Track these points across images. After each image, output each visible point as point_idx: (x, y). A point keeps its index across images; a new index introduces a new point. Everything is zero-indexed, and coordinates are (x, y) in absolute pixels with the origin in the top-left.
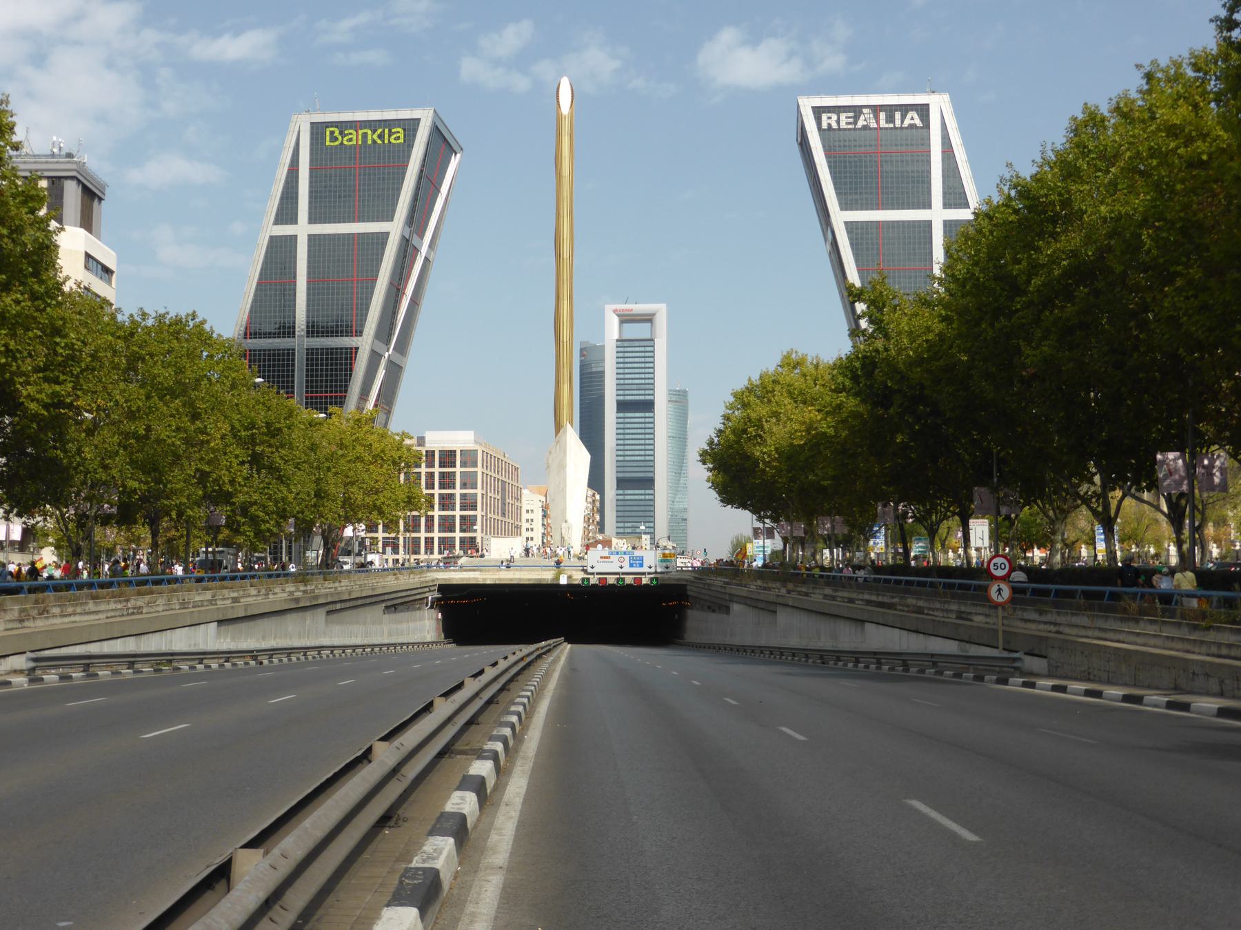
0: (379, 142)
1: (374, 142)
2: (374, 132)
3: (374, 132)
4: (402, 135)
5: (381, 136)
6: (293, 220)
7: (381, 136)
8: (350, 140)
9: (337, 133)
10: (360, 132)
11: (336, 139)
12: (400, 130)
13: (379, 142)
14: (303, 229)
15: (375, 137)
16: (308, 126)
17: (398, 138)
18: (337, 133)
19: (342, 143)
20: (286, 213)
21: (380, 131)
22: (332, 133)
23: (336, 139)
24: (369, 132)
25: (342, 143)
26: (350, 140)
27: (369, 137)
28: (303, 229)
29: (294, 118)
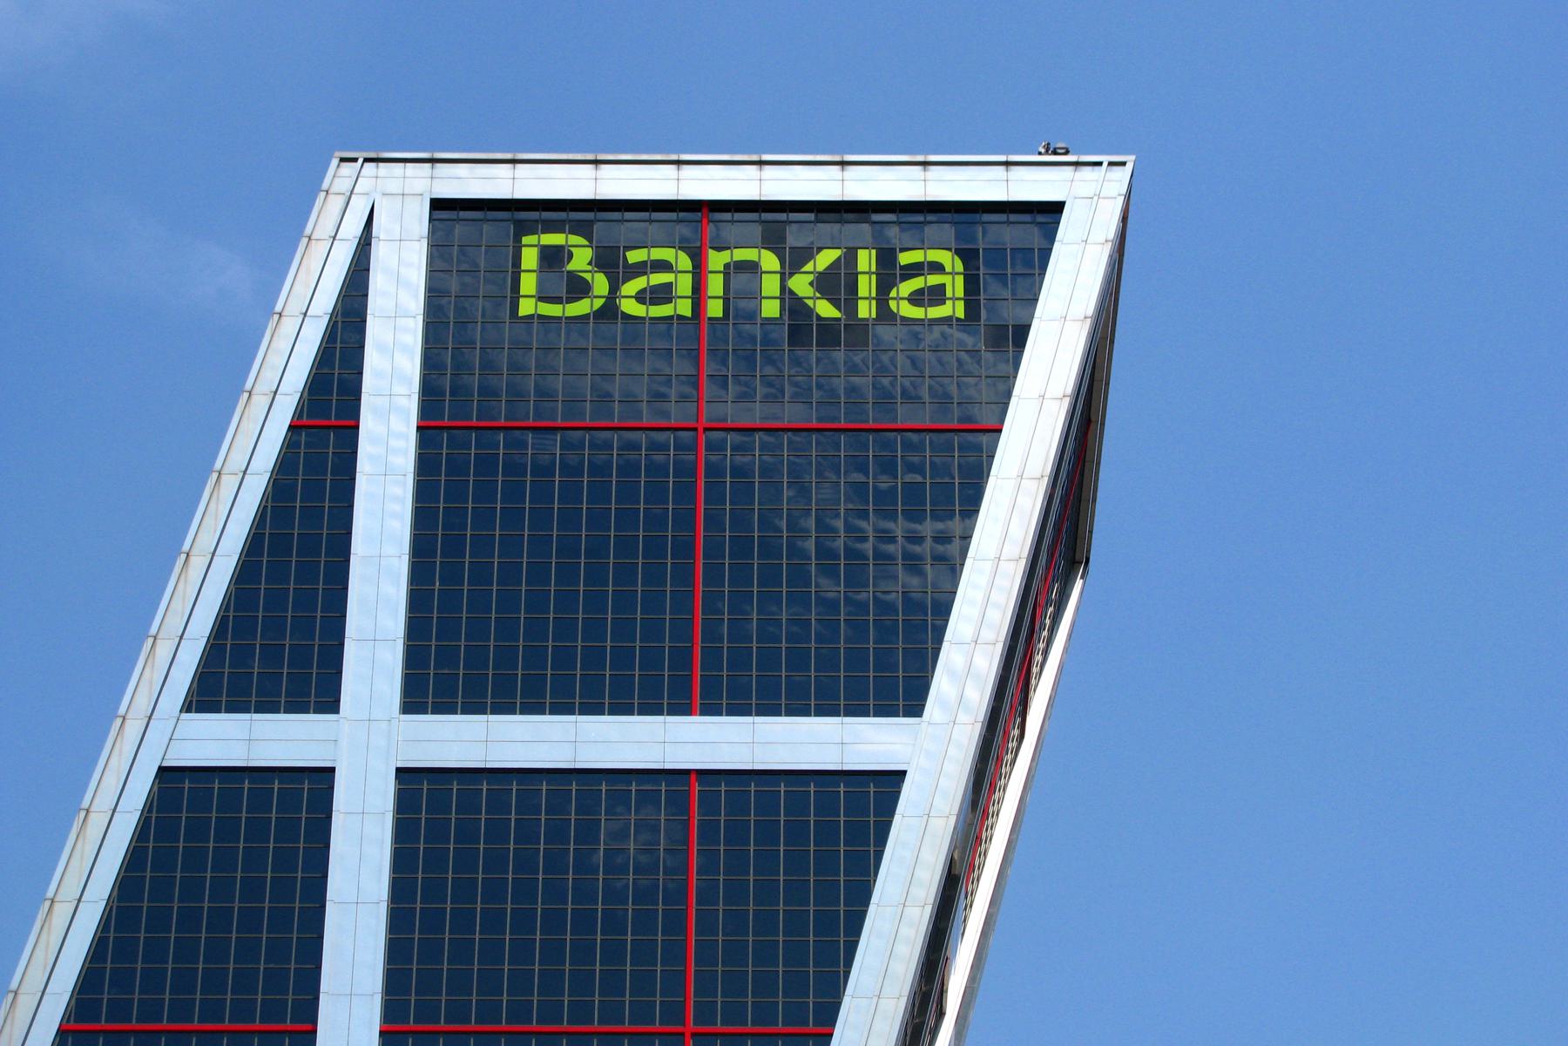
0: (825, 309)
1: (794, 306)
2: (794, 262)
3: (794, 262)
4: (956, 286)
5: (837, 284)
6: (318, 689)
7: (827, 284)
8: (662, 294)
9: (581, 258)
10: (716, 260)
11: (579, 288)
12: (944, 257)
13: (825, 309)
14: (368, 739)
15: (801, 285)
16: (418, 220)
17: (936, 295)
18: (581, 258)
19: (609, 310)
20: (275, 640)
21: (825, 259)
22: (552, 258)
23: (579, 288)
24: (770, 261)
25: (609, 310)
26: (662, 294)
27: (771, 285)
28: (368, 739)
29: (340, 177)
